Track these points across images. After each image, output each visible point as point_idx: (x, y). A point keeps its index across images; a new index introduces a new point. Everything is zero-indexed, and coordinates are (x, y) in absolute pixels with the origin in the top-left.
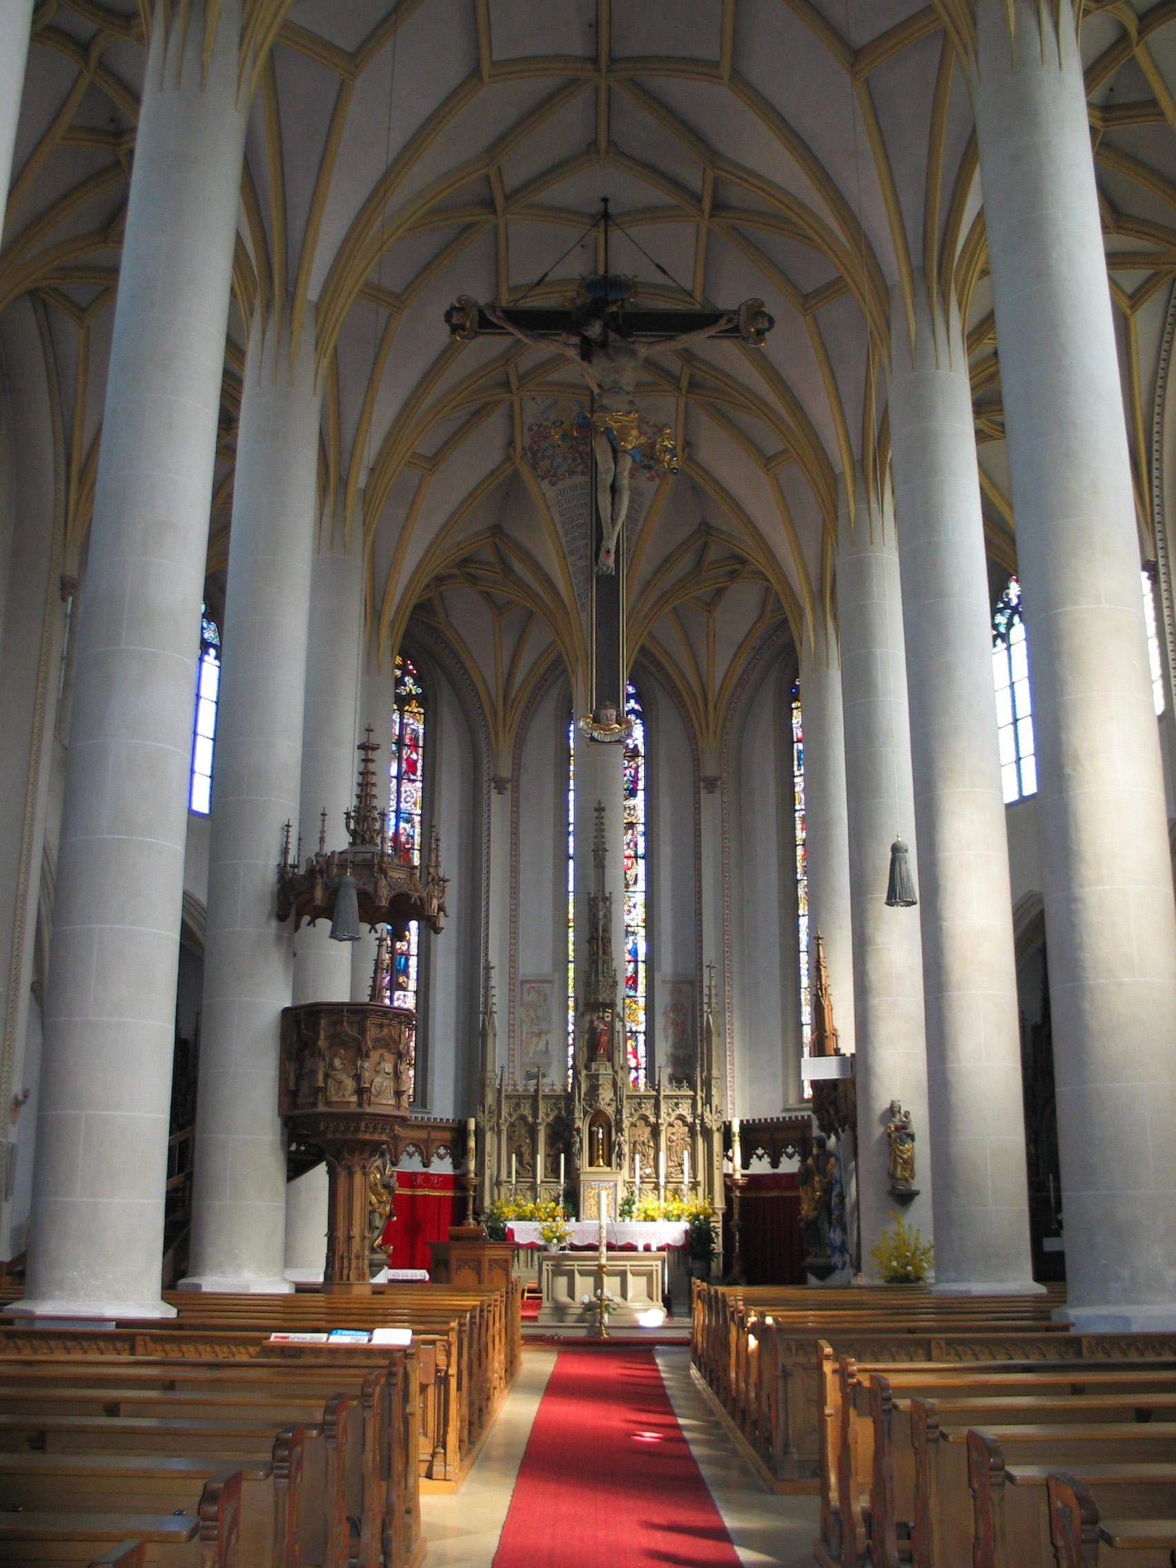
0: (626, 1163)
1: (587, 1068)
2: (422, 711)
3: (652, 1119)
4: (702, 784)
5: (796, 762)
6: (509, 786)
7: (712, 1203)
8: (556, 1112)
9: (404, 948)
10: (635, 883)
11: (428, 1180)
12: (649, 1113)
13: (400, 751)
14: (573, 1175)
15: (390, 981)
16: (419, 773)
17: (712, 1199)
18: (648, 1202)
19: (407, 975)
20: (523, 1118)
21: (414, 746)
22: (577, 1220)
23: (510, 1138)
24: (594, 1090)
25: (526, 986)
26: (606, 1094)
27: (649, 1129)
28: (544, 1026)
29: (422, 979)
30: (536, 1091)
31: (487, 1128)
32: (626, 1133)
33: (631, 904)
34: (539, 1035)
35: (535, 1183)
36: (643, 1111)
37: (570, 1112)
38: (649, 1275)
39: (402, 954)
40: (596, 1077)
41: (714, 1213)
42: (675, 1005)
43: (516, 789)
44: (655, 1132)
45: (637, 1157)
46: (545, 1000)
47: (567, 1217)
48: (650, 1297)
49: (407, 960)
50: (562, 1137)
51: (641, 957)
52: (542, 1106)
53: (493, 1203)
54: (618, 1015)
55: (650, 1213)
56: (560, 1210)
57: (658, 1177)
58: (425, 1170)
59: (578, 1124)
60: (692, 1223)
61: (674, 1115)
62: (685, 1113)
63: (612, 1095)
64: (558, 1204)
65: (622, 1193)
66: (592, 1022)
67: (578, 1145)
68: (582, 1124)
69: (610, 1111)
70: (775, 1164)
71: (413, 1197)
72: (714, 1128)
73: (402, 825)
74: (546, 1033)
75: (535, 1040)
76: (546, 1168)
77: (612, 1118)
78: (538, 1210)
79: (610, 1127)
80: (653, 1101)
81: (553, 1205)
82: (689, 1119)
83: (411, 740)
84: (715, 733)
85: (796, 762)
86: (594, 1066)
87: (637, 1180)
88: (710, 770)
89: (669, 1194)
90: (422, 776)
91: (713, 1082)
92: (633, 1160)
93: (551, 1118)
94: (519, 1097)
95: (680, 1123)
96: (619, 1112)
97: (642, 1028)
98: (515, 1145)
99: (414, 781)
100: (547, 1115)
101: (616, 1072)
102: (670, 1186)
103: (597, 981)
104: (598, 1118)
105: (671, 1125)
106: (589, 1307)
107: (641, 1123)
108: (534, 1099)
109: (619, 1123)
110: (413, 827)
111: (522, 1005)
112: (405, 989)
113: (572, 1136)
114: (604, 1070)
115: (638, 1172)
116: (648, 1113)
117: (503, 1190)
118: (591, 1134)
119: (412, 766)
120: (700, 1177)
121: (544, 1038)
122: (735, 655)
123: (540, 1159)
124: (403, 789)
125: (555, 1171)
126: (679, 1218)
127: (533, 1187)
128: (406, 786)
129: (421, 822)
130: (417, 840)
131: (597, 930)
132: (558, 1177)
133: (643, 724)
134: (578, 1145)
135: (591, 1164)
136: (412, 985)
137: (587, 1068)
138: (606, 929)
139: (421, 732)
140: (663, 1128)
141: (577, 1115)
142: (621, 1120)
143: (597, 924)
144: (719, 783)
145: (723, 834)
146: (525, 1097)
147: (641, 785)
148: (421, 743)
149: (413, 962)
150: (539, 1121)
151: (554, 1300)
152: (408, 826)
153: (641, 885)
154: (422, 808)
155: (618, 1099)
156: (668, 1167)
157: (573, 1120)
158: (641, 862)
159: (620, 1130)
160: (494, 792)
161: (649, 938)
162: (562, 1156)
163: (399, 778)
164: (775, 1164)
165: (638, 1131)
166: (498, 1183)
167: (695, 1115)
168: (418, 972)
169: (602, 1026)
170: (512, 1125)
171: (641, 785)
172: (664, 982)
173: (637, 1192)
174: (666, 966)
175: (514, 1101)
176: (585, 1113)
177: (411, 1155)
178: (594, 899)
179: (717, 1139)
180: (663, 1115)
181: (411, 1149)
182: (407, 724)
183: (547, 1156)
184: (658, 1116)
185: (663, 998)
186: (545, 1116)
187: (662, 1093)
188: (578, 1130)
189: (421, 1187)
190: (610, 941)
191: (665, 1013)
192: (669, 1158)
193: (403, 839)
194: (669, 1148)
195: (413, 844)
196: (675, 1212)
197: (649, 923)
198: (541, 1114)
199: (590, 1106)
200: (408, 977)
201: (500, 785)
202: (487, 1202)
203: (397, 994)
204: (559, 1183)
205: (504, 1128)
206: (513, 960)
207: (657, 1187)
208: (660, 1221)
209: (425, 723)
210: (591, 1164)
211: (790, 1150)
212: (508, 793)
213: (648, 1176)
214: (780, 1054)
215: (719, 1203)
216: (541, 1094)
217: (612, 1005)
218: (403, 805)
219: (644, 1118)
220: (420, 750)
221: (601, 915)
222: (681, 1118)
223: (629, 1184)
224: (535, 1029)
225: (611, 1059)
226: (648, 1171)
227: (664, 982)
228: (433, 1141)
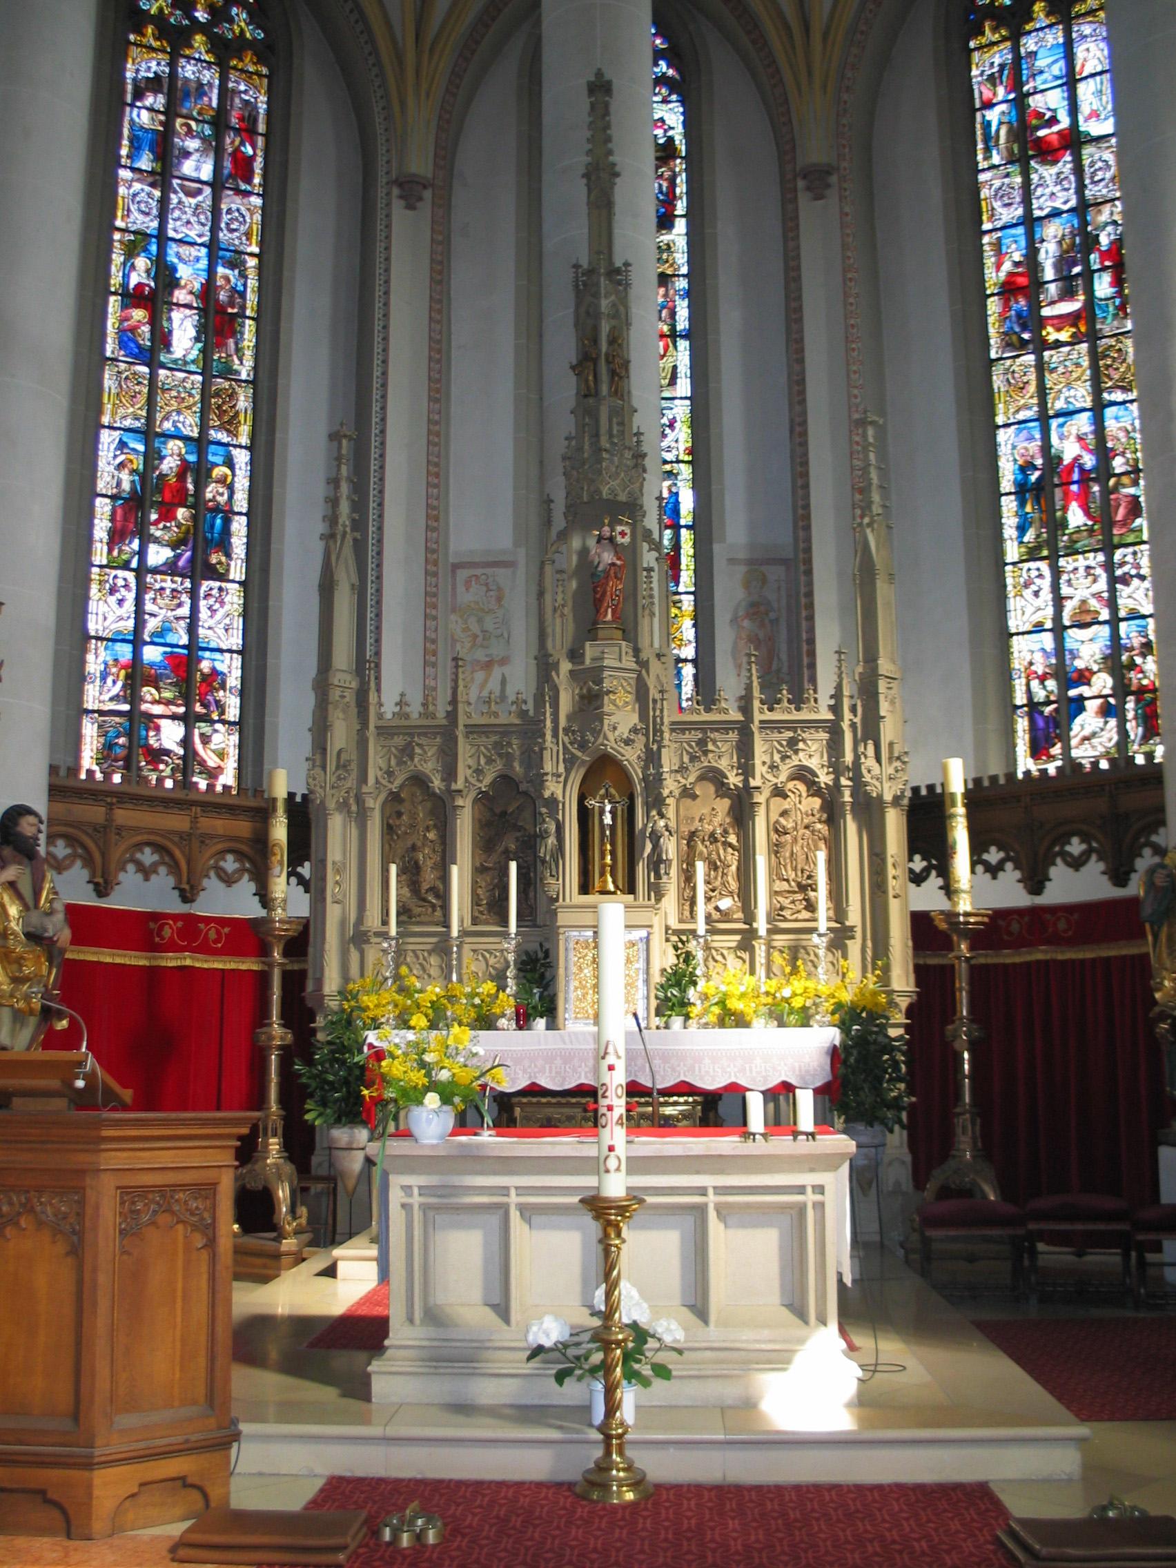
0: (672, 883)
1: (575, 655)
2: (265, 71)
3: (734, 779)
4: (801, 184)
5: (980, 146)
6: (427, 194)
7: (885, 979)
8: (499, 765)
9: (222, 500)
10: (673, 381)
11: (192, 931)
12: (726, 763)
13: (218, 136)
14: (539, 912)
15: (192, 560)
16: (257, 180)
17: (886, 969)
18: (726, 978)
19: (226, 550)
20: (419, 781)
21: (248, 131)
22: (552, 1026)
23: (389, 829)
24: (591, 703)
25: (462, 574)
26: (621, 717)
27: (726, 803)
28: (497, 650)
29: (256, 561)
30: (452, 716)
31: (331, 805)
32: (671, 812)
33: (665, 421)
34: (488, 665)
35: (447, 934)
36: (711, 760)
37: (533, 759)
38: (795, 1221)
39: (217, 509)
40: (596, 674)
41: (892, 1004)
42: (753, 605)
43: (444, 203)
44: (742, 809)
45: (700, 867)
46: (499, 599)
47: (523, 1020)
48: (798, 1310)
49: (227, 522)
50: (512, 823)
51: (686, 518)
52: (464, 750)
53: (346, 978)
54: (648, 534)
55: (734, 1004)
56: (507, 1002)
57: (749, 918)
58: (182, 908)
59: (553, 788)
60: (844, 1026)
61: (785, 771)
62: (814, 763)
63: (634, 719)
64: (502, 987)
65: (664, 958)
66: (584, 552)
67: (552, 841)
68: (562, 789)
69: (631, 757)
70: (1035, 883)
71: (153, 972)
72: (888, 797)
73: (221, 270)
74: (504, 661)
75: (480, 676)
76: (476, 901)
77: (636, 773)
78: (452, 998)
79: (631, 798)
80: (733, 736)
81: (489, 987)
82: (824, 778)
83: (241, 119)
84: (824, 87)
85: (980, 146)
86: (590, 651)
87: (701, 928)
88: (815, 150)
89: (778, 960)
90: (264, 185)
91: (882, 685)
92: (688, 877)
93: (488, 780)
94: (411, 732)
95: (802, 788)
96: (652, 758)
97: (689, 652)
98: (401, 847)
99: (247, 194)
100: (479, 772)
101: (644, 664)
102: (781, 940)
103: (598, 450)
104: (602, 770)
105: (779, 792)
106: (563, 1361)
107: (706, 790)
108: (447, 736)
109: (654, 783)
110: (243, 276)
111: (454, 610)
112: (223, 577)
113: (536, 817)
114: (614, 658)
115: (701, 908)
116: (723, 764)
117: (372, 955)
118: (584, 815)
119: (243, 167)
120: (854, 917)
121: (497, 672)
123: (459, 879)
124: (224, 207)
125: (498, 909)
126: (805, 1018)
127: (443, 948)
128: (231, 202)
129: (260, 268)
130: (252, 298)
131: (595, 341)
132: (505, 922)
133: (682, 102)
134: (552, 841)
135: (585, 889)
136: (237, 571)
137: (575, 655)
138: (617, 340)
139: (262, 107)
140: (760, 798)
141: (548, 767)
142: (659, 779)
143: (596, 329)
144: (834, 179)
145: (845, 271)
146: (425, 731)
147: (681, 207)
148: (261, 128)
149: (239, 526)
150: (460, 784)
151: (434, 1317)
152: (232, 274)
153: (684, 387)
154: (261, 244)
155: (649, 727)
156: (774, 893)
157: (539, 781)
158: (683, 345)
159: (656, 803)
160: (398, 207)
161: (701, 484)
162: (513, 866)
163: (217, 185)
164: (1035, 883)
165: (699, 809)
166: (358, 938)
167: (836, 767)
168: (249, 545)
169: (608, 557)
170: (394, 797)
171: (681, 207)
172: (732, 561)
173: (700, 955)
174: (735, 533)
175: (399, 741)
176: (570, 762)
177: (146, 872)
178: (591, 272)
179: (894, 825)
180: (760, 769)
181: (148, 857)
182: (235, 92)
183: (479, 870)
184: (746, 769)
185: (730, 592)
186: (473, 771)
187: (757, 717)
188: (552, 803)
189: (172, 947)
190: (626, 364)
191: (734, 621)
192: (775, 874)
193: (223, 296)
194: (775, 849)
195: (243, 308)
196: (797, 1003)
197: (700, 455)
198: (463, 772)
199: (583, 746)
200: (228, 555)
201: (410, 189)
202: (331, 984)
203: (205, 585)
204: (505, 935)
205: (374, 805)
206: (435, 517)
207: (747, 940)
208: (758, 1023)
209: (269, 92)
210: (585, 889)
211: (1076, 847)
212: (426, 207)
213: (726, 916)
214: (967, 695)
215: (902, 981)
216: (462, 720)
217: (633, 509)
218: (224, 236)
219: (715, 777)
220: (260, 141)
221: (605, 304)
222: (803, 775)
223: (680, 938)
224: (480, 655)
225: (629, 633)
226: (725, 903)
227: (732, 561)
228: (205, 839)
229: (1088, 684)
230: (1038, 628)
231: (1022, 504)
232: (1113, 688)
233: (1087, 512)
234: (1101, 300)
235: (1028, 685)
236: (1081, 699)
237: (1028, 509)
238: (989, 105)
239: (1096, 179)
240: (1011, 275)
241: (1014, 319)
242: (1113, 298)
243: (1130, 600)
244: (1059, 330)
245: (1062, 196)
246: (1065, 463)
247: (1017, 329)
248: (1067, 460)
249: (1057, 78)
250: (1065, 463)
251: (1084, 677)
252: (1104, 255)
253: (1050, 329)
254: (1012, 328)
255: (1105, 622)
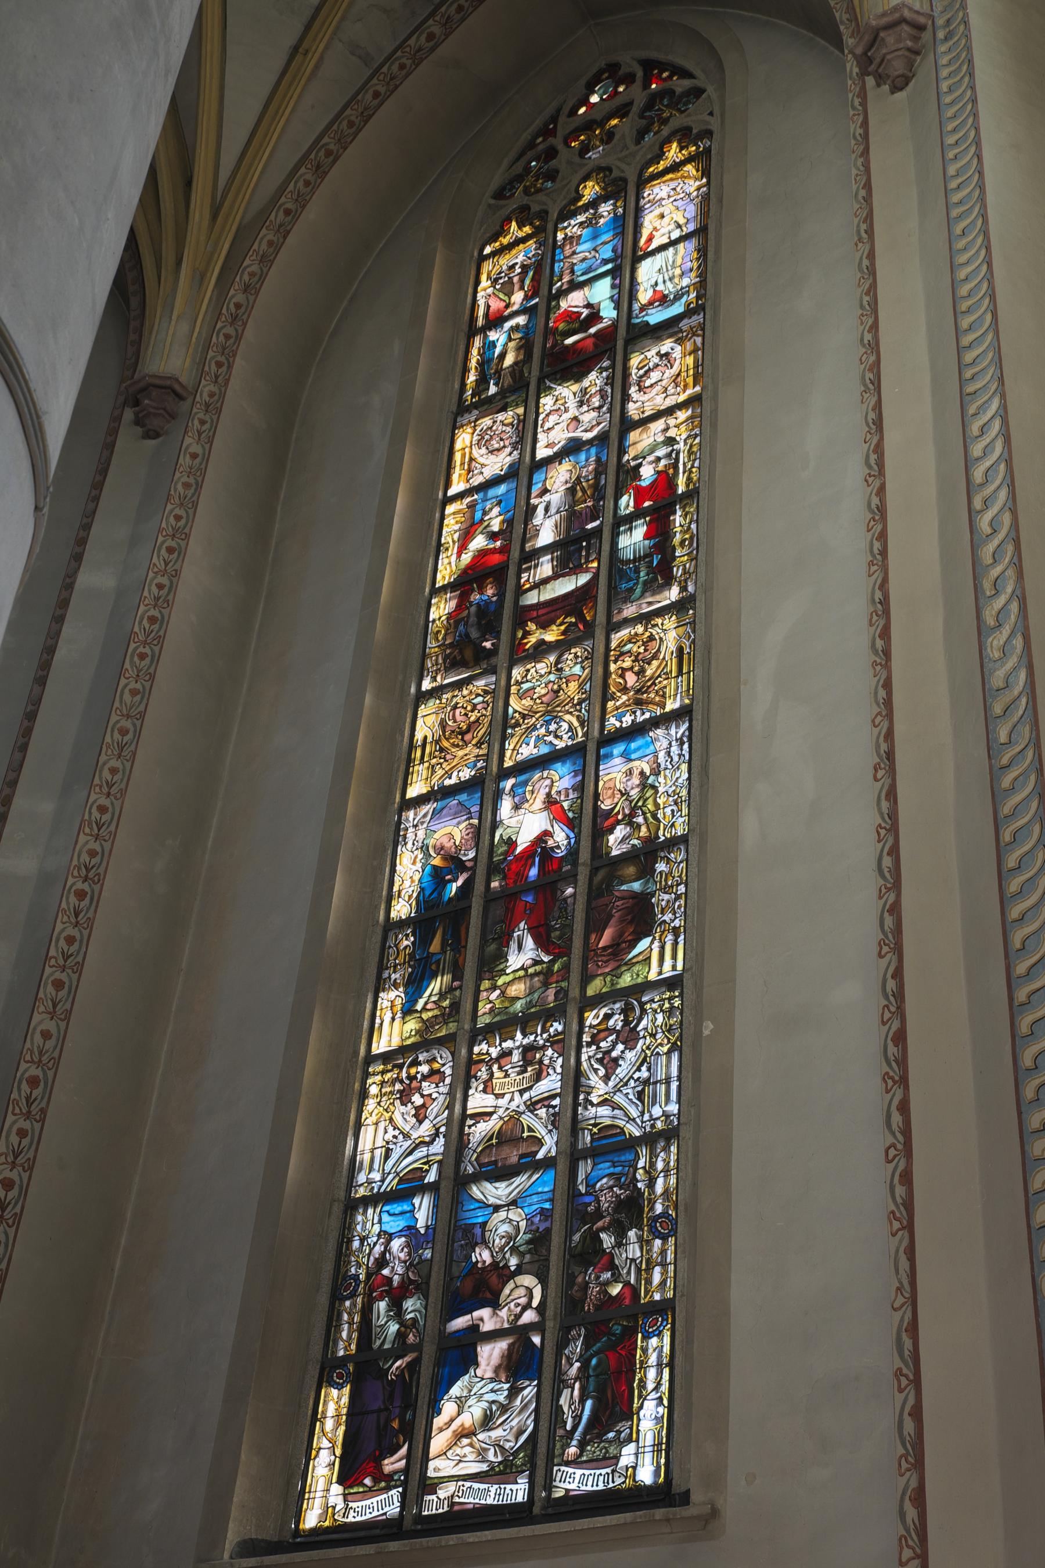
122: (295, 50)
229: (495, 1304)
230: (410, 1187)
231: (423, 940)
232: (541, 1309)
233: (542, 943)
234: (629, 561)
235: (367, 1312)
236: (475, 1336)
237: (435, 946)
238: (495, 321)
239: (648, 383)
240: (482, 553)
241: (473, 619)
242: (646, 556)
243: (604, 1111)
244: (544, 626)
245: (589, 417)
246: (519, 850)
247: (474, 634)
248: (523, 841)
249: (605, 262)
250: (519, 850)
251: (486, 1288)
252: (641, 494)
253: (531, 626)
254: (467, 635)
255: (548, 1163)
